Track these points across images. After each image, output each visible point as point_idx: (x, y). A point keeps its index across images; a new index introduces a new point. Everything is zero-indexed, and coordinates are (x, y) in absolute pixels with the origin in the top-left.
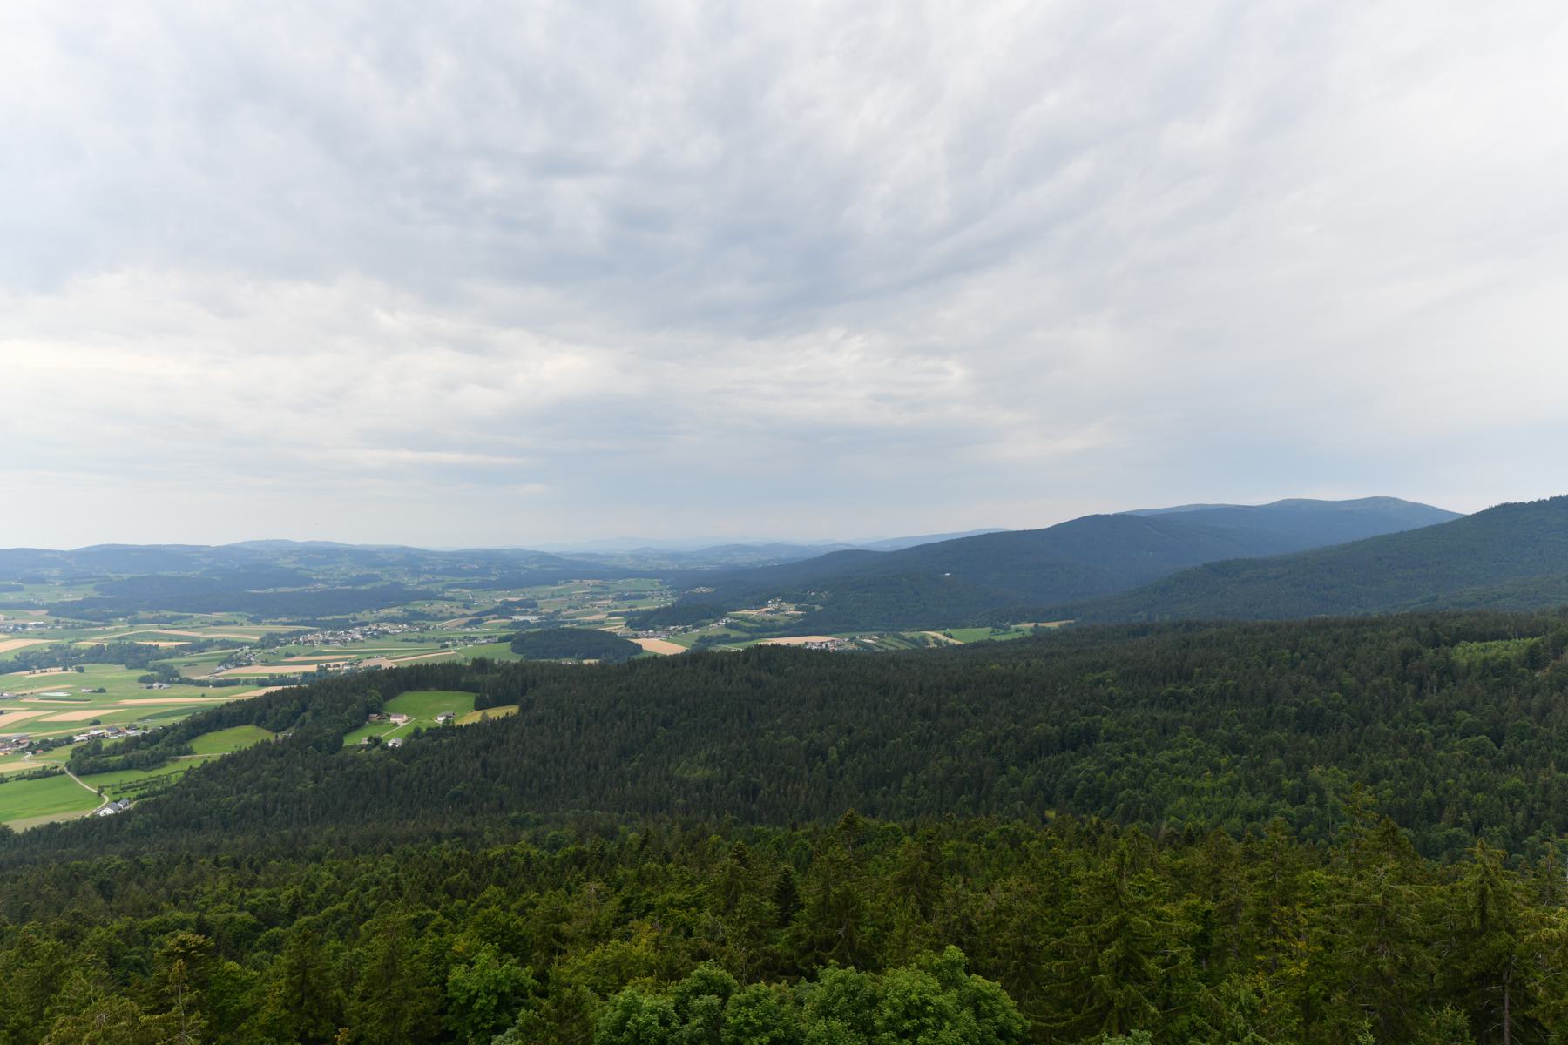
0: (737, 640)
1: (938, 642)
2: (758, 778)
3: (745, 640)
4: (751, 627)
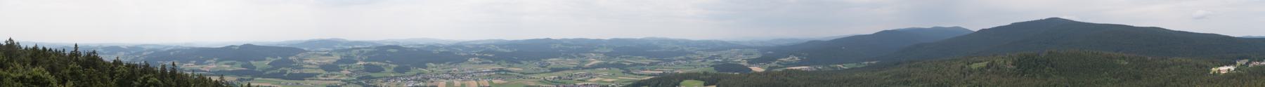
0: (781, 68)
1: (841, 68)
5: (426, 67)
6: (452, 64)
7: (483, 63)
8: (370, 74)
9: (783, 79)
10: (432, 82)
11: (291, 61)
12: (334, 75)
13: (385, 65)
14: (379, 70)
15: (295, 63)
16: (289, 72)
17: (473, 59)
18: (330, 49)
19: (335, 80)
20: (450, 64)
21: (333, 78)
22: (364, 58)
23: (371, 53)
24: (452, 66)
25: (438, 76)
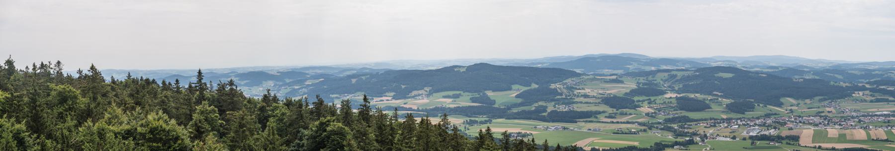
5: (780, 105)
6: (825, 100)
7: (878, 101)
8: (685, 113)
10: (791, 129)
11: (555, 92)
12: (626, 114)
13: (711, 100)
14: (702, 106)
15: (561, 94)
16: (550, 108)
17: (861, 93)
18: (620, 72)
19: (628, 123)
20: (820, 101)
21: (624, 119)
22: (676, 88)
23: (688, 78)
24: (826, 103)
25: (800, 120)
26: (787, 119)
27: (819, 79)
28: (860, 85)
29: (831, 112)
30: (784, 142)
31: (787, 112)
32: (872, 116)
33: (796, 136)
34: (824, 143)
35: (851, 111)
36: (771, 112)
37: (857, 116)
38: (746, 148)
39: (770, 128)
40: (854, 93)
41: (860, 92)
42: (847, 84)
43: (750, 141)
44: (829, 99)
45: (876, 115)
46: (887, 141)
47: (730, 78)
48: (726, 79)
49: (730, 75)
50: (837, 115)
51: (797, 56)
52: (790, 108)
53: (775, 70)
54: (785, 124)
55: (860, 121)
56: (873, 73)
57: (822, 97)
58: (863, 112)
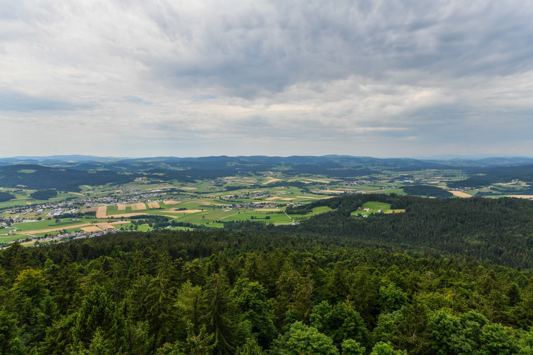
2: (502, 248)
3: (500, 195)
4: (503, 190)
5: (79, 191)
6: (114, 185)
7: (152, 183)
9: (500, 210)
10: (89, 207)
17: (140, 179)
20: (111, 186)
24: (115, 187)
25: (95, 200)
26: (85, 201)
27: (108, 171)
28: (140, 173)
29: (120, 192)
30: (84, 217)
31: (85, 195)
32: (149, 193)
33: (93, 212)
34: (115, 214)
35: (134, 191)
36: (71, 197)
37: (139, 194)
38: (51, 225)
39: (71, 208)
40: (136, 179)
41: (139, 178)
42: (130, 173)
43: (55, 220)
44: (116, 184)
45: (152, 193)
46: (160, 209)
47: (33, 173)
48: (29, 174)
49: (33, 171)
50: (124, 195)
51: (90, 155)
52: (87, 192)
53: (73, 166)
54: (84, 204)
55: (141, 197)
56: (148, 165)
57: (112, 183)
58: (142, 191)
